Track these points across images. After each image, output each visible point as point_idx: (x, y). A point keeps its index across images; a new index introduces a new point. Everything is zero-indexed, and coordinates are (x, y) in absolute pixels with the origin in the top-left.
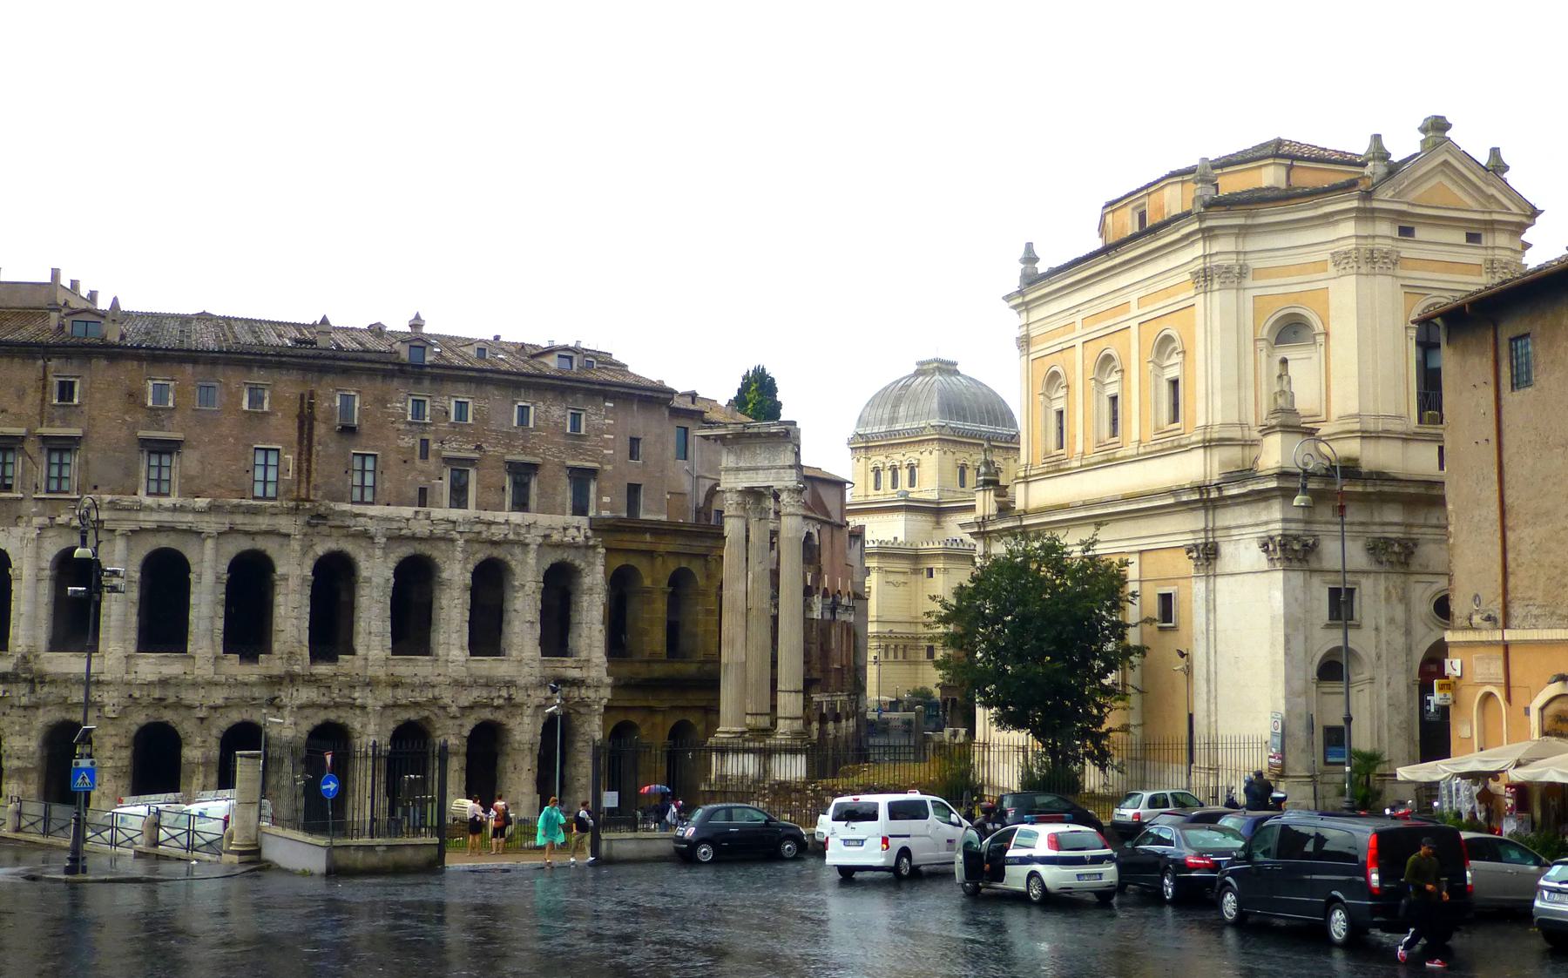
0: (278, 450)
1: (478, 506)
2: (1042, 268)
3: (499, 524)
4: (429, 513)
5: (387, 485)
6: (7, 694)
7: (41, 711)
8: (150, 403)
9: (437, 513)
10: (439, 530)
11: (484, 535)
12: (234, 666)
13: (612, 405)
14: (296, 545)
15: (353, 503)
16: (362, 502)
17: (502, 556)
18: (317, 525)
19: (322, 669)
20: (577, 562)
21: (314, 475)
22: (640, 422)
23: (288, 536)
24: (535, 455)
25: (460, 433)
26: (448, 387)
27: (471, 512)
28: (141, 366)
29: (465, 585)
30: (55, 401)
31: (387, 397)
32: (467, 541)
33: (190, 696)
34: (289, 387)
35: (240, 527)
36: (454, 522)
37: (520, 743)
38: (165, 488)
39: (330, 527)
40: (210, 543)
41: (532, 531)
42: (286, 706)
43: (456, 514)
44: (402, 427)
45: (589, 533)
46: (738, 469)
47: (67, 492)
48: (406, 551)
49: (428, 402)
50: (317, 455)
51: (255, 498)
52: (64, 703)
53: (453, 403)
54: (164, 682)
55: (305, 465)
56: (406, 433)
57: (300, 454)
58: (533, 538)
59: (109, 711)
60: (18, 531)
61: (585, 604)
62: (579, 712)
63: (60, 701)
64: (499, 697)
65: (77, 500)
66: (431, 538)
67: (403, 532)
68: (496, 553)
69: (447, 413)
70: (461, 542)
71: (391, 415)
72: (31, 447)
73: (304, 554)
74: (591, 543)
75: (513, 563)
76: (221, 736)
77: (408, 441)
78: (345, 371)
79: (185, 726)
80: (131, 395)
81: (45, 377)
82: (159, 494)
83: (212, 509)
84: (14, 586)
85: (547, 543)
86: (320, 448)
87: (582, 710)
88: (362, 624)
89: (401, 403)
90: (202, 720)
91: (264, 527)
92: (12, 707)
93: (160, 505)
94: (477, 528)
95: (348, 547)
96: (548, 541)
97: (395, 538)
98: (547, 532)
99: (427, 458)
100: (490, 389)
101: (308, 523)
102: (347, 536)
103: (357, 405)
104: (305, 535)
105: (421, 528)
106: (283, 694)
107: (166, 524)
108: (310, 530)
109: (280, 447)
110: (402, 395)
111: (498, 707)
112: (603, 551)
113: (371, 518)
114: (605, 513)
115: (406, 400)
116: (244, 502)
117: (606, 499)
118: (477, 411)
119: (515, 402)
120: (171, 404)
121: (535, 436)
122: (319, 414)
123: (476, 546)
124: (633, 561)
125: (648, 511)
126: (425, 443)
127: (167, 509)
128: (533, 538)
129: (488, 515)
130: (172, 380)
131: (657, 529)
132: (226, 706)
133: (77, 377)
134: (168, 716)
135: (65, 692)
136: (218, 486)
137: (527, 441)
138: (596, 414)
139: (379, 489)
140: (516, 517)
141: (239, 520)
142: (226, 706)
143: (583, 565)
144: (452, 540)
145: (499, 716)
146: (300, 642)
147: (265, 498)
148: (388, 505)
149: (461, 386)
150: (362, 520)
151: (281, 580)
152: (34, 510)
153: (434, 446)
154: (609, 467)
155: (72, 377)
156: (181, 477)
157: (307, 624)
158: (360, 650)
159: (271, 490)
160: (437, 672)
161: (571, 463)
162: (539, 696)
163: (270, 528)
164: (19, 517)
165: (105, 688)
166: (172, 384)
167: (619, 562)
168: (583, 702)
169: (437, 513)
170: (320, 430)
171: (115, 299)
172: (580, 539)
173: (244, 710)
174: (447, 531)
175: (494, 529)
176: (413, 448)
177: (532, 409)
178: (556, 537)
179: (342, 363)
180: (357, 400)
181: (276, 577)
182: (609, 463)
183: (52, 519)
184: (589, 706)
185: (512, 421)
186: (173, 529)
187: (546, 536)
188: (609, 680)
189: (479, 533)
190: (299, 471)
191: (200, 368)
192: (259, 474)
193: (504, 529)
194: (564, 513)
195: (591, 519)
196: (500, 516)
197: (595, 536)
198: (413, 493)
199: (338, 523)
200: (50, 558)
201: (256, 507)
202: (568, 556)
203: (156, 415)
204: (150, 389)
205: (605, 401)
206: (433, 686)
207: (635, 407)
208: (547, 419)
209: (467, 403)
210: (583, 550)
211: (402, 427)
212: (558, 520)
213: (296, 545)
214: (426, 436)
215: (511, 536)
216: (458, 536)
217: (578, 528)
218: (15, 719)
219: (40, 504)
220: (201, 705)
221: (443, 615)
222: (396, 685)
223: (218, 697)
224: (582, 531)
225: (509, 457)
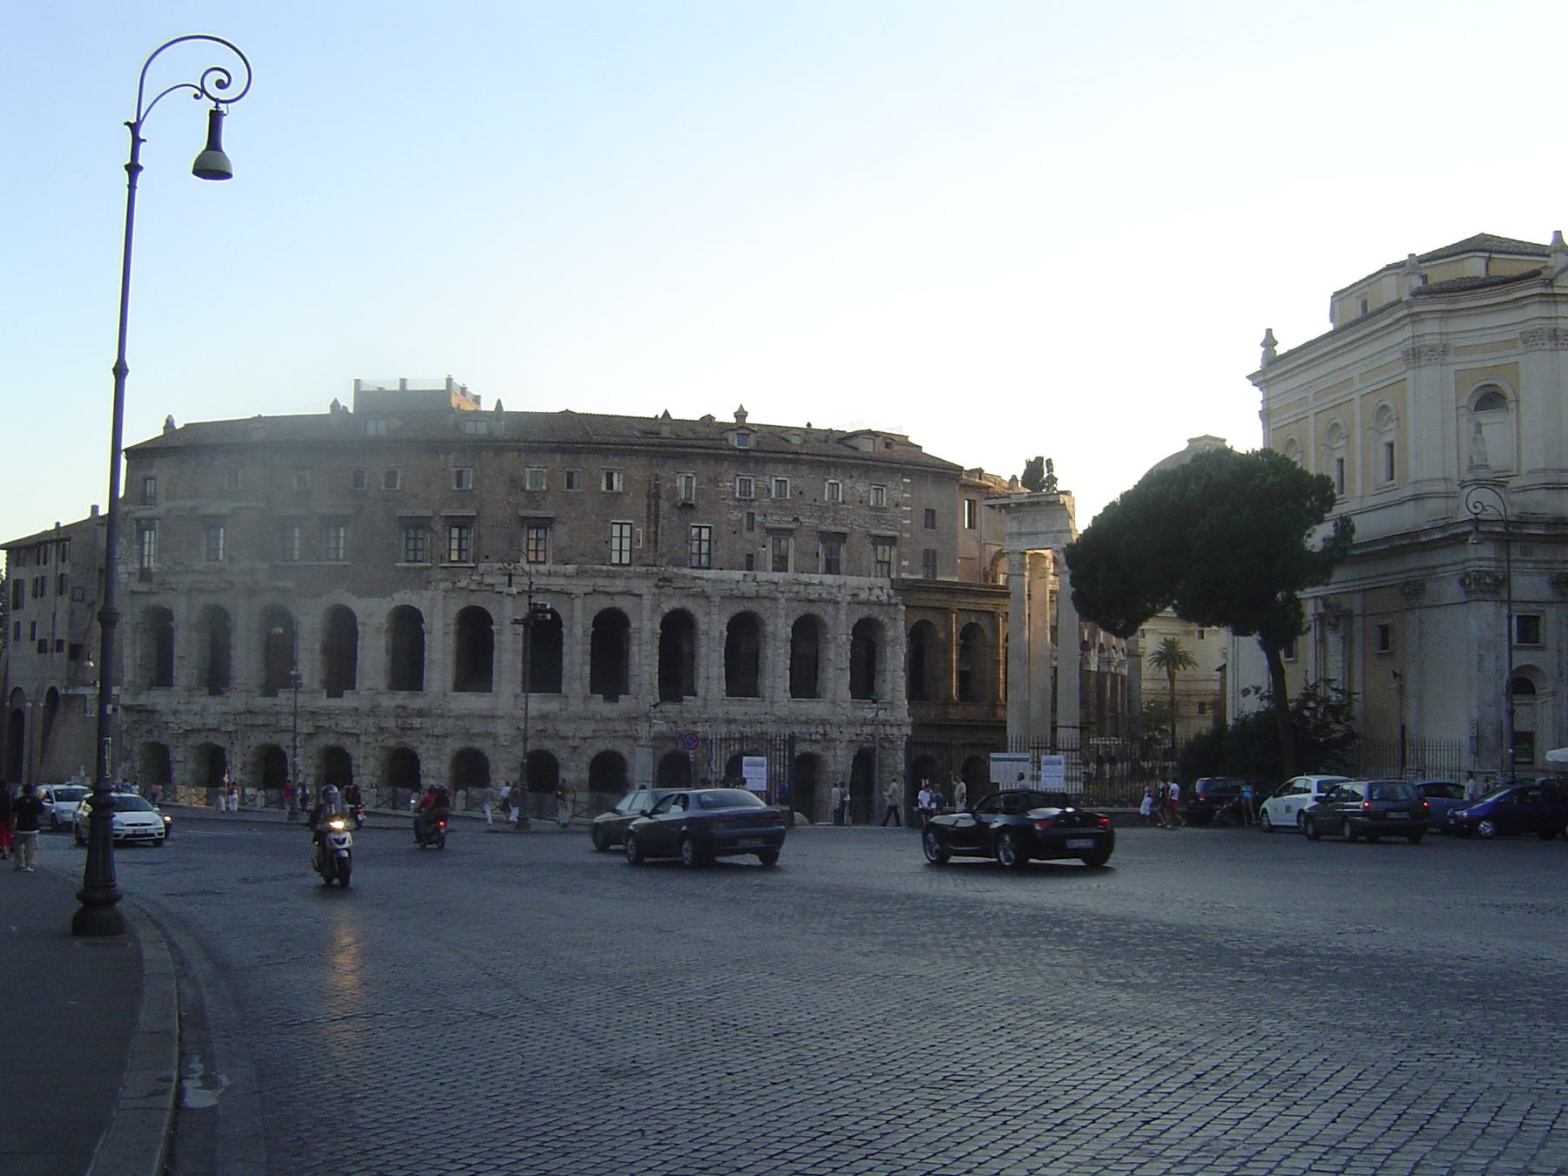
0: (630, 524)
1: (796, 570)
2: (1280, 350)
3: (814, 584)
4: (755, 576)
5: (720, 552)
7: (449, 740)
8: (528, 488)
9: (761, 576)
10: (763, 592)
11: (803, 594)
12: (599, 705)
13: (908, 481)
14: (647, 602)
15: (692, 568)
16: (700, 567)
17: (816, 613)
18: (663, 586)
19: (670, 708)
20: (881, 618)
21: (660, 544)
22: (932, 495)
24: (844, 526)
25: (780, 508)
26: (770, 467)
27: (790, 575)
29: (787, 637)
31: (719, 478)
32: (787, 600)
33: (566, 729)
34: (638, 469)
36: (776, 584)
37: (833, 772)
38: (541, 558)
40: (578, 602)
41: (843, 591)
43: (777, 576)
44: (731, 503)
45: (891, 592)
46: (1020, 534)
47: (465, 562)
48: (739, 608)
49: (753, 482)
51: (613, 565)
52: (468, 734)
53: (774, 482)
54: (544, 717)
55: (653, 537)
56: (736, 508)
57: (648, 527)
58: (844, 597)
59: (501, 739)
60: (427, 594)
61: (888, 654)
62: (883, 747)
63: (464, 731)
64: (817, 733)
65: (472, 567)
66: (758, 597)
67: (734, 592)
68: (814, 609)
70: (783, 601)
71: (721, 493)
72: (438, 526)
73: (654, 611)
74: (893, 601)
75: (827, 620)
76: (589, 760)
77: (736, 515)
78: (684, 456)
79: (562, 755)
80: (512, 481)
82: (537, 562)
83: (579, 574)
84: (426, 637)
85: (855, 601)
86: (665, 522)
87: (886, 745)
88: (701, 670)
89: (730, 483)
90: (574, 747)
91: (620, 589)
92: (427, 736)
93: (537, 571)
94: (795, 588)
95: (689, 605)
96: (856, 599)
97: (729, 597)
98: (855, 592)
99: (753, 530)
100: (804, 470)
101: (656, 586)
102: (687, 596)
103: (694, 484)
104: (654, 595)
105: (749, 588)
106: (638, 728)
107: (543, 587)
108: (655, 590)
110: (732, 476)
111: (816, 741)
112: (903, 608)
113: (707, 580)
114: (904, 575)
115: (735, 480)
116: (604, 568)
117: (905, 563)
118: (794, 488)
119: (827, 480)
120: (544, 488)
121: (843, 509)
122: (663, 495)
123: (795, 604)
124: (929, 616)
125: (943, 574)
126: (751, 516)
127: (543, 575)
128: (844, 597)
129: (805, 577)
131: (950, 590)
132: (594, 738)
133: (470, 467)
134: (548, 745)
135: (468, 725)
136: (583, 555)
137: (836, 512)
138: (895, 489)
139: (713, 556)
140: (829, 579)
141: (600, 582)
142: (594, 738)
143: (886, 620)
144: (775, 599)
145: (816, 749)
146: (651, 684)
147: (621, 564)
149: (781, 468)
150: (700, 582)
153: (758, 519)
154: (907, 535)
156: (554, 548)
157: (657, 670)
158: (701, 692)
159: (626, 560)
160: (763, 711)
161: (874, 532)
162: (849, 733)
163: (625, 590)
164: (429, 582)
165: (500, 721)
166: (545, 470)
167: (917, 617)
168: (887, 738)
169: (761, 576)
170: (664, 506)
171: (499, 402)
172: (884, 598)
173: (607, 741)
174: (770, 592)
175: (810, 589)
176: (741, 519)
177: (841, 485)
178: (863, 596)
179: (680, 449)
180: (694, 480)
181: (631, 631)
182: (907, 532)
183: (454, 583)
184: (892, 742)
185: (823, 495)
186: (548, 591)
187: (854, 595)
188: (909, 720)
189: (797, 593)
190: (648, 540)
191: (566, 457)
192: (615, 544)
193: (819, 589)
194: (870, 576)
195: (892, 580)
196: (816, 578)
197: (896, 595)
198: (742, 559)
200: (454, 616)
201: (614, 572)
202: (875, 612)
203: (533, 498)
204: (528, 475)
205: (903, 478)
206: (761, 723)
207: (929, 484)
208: (853, 494)
209: (785, 481)
210: (886, 608)
211: (731, 503)
212: (864, 581)
213: (647, 602)
214: (752, 511)
215: (824, 595)
216: (780, 595)
217: (882, 588)
219: (444, 570)
220: (574, 736)
221: (769, 662)
222: (730, 722)
223: (588, 729)
224: (885, 591)
225: (824, 528)
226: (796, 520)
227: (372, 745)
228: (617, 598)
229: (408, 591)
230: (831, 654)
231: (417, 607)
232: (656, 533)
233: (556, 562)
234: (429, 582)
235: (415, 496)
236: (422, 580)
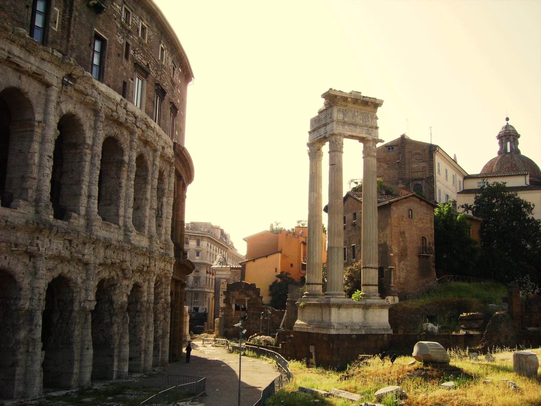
21: (72, 36)
23: (48, 86)
35: (17, 60)
36: (136, 118)
39: (75, 89)
42: (41, 255)
50: (75, 20)
57: (64, 12)
69: (138, 30)
106: (39, 242)
126: (128, 45)
141: (16, 50)
148: (109, 86)
151: (39, 126)
153: (132, 52)
158: (83, 211)
175: (150, 132)
190: (62, 26)
198: (121, 84)
199: (81, 88)
226: (148, 65)
228: (24, 78)
230: (148, 196)
232: (70, 22)
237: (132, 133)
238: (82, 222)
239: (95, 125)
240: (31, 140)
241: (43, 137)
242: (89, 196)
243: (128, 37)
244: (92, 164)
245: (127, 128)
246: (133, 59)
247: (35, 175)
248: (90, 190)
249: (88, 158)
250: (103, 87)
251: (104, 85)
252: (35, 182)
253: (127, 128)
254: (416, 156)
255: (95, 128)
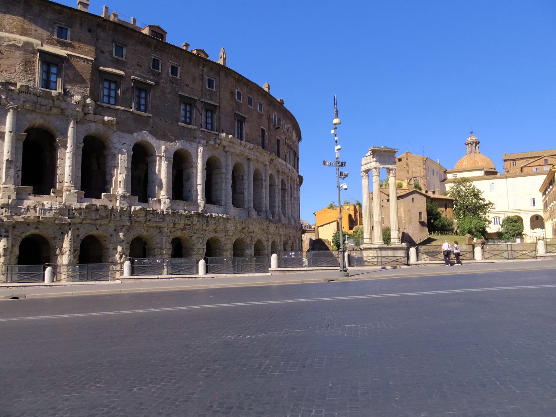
6: (198, 223)
8: (237, 98)
28: (234, 81)
30: (207, 87)
35: (258, 159)
65: (216, 135)
81: (202, 75)
109: (265, 129)
126: (285, 138)
130: (242, 91)
152: (201, 136)
155: (212, 78)
158: (277, 213)
204: (237, 92)
218: (200, 235)
227: (169, 235)
229: (185, 141)
231: (189, 151)
233: (246, 141)
234: (195, 138)
235: (187, 85)
236: (190, 137)
237: (288, 177)
238: (277, 218)
239: (278, 176)
240: (262, 188)
241: (266, 186)
242: (278, 207)
243: (285, 135)
244: (278, 193)
245: (287, 175)
246: (287, 143)
247: (264, 202)
248: (278, 205)
249: (277, 191)
250: (280, 160)
251: (280, 159)
252: (264, 205)
253: (287, 175)
254: (415, 164)
255: (278, 178)
